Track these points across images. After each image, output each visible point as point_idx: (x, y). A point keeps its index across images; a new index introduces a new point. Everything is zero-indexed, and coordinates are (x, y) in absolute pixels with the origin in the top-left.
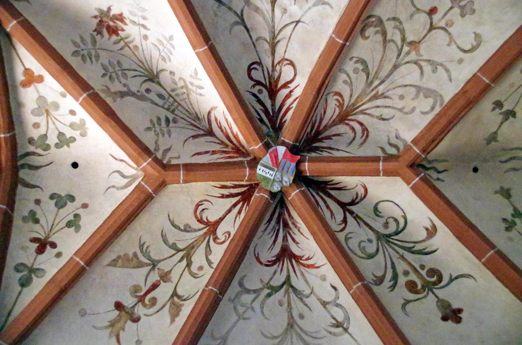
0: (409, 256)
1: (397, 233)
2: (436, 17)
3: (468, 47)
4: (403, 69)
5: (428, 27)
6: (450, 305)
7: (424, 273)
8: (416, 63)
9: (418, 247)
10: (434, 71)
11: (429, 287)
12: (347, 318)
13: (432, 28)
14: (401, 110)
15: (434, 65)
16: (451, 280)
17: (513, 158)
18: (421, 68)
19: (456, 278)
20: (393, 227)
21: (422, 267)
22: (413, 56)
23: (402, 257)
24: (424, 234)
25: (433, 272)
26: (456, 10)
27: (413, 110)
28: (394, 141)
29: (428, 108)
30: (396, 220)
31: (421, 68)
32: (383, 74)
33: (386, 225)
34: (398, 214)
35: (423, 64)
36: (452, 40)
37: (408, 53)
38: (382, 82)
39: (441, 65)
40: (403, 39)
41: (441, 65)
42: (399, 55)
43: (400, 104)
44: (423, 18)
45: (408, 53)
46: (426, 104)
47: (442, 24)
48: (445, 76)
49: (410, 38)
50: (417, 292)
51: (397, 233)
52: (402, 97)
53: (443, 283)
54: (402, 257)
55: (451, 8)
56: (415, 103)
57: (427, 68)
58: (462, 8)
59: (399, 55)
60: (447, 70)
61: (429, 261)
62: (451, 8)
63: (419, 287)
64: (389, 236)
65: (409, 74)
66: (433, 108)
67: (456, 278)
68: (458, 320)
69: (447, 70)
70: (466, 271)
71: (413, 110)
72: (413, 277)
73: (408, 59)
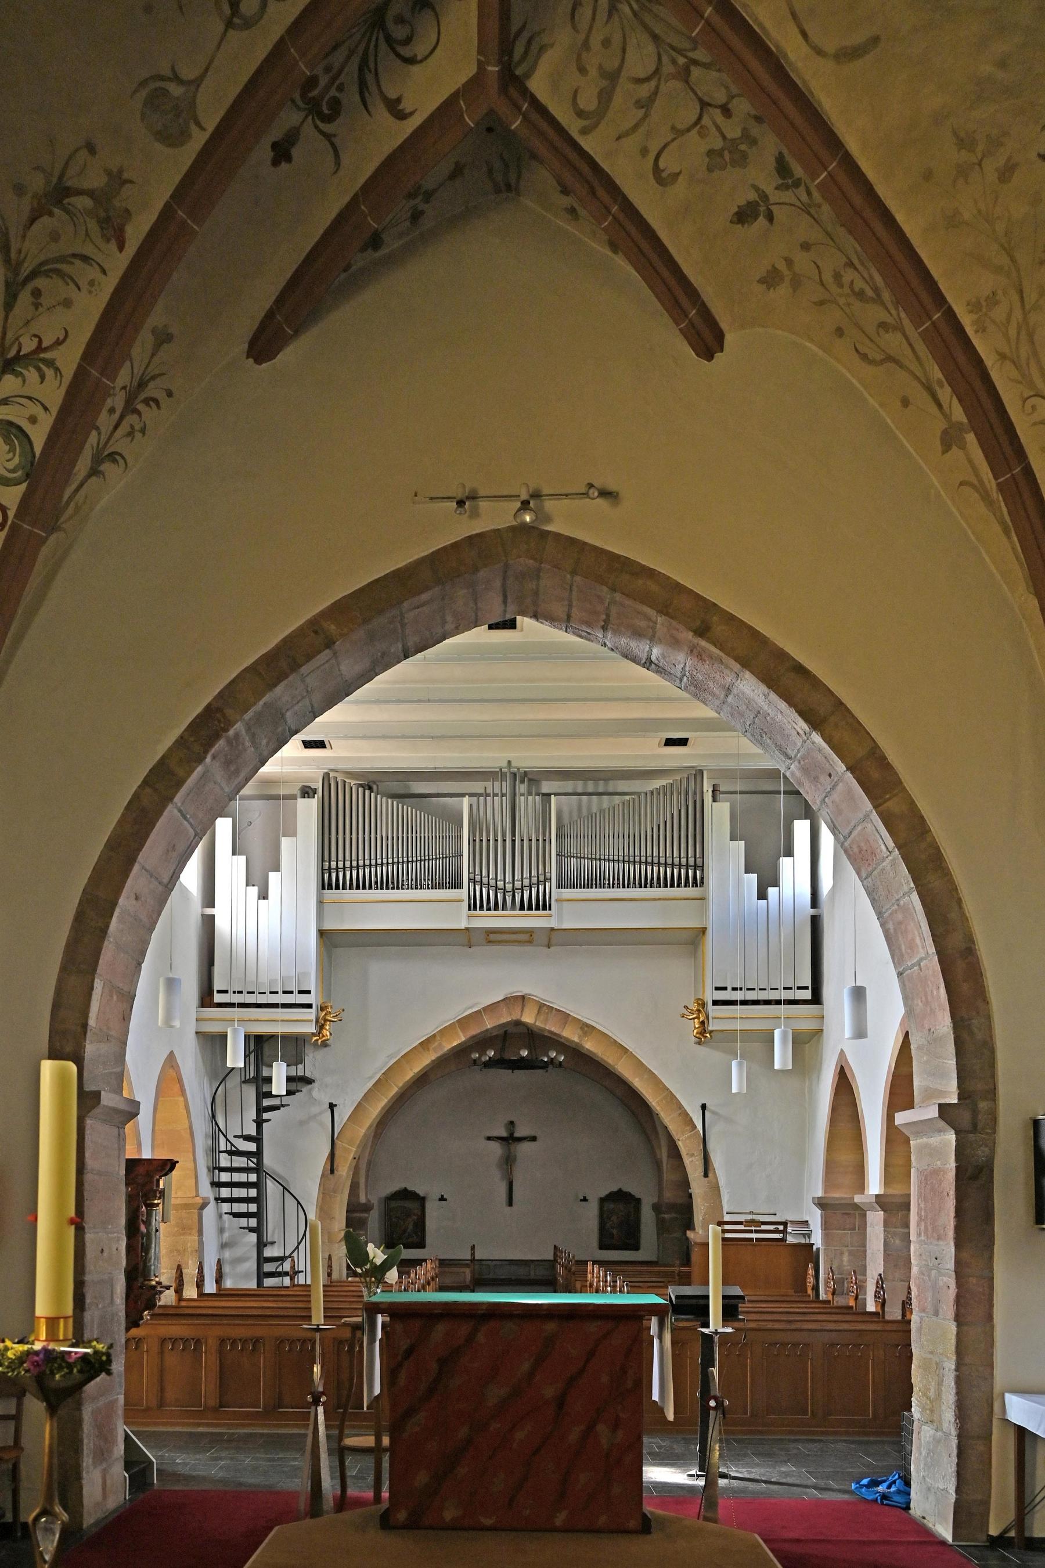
0: (356, 61)
1: (389, 39)
2: (717, 114)
3: (662, 164)
4: (651, 48)
5: (706, 99)
6: (293, 144)
7: (333, 92)
8: (657, 71)
9: (370, 78)
10: (639, 104)
11: (313, 108)
12: (248, 24)
13: (704, 105)
14: (586, 45)
15: (646, 104)
16: (328, 137)
17: (507, 166)
18: (647, 79)
19: (332, 144)
20: (399, 32)
21: (341, 88)
22: (668, 68)
23: (352, 52)
24: (392, 95)
25: (336, 106)
26: (718, 144)
27: (582, 70)
28: (534, 48)
29: (582, 104)
30: (408, 41)
31: (647, 79)
32: (648, 19)
33: (400, 20)
34: (420, 49)
35: (653, 83)
36: (679, 133)
37: (674, 62)
38: (635, 14)
39: (646, 116)
40: (695, 62)
41: (646, 116)
42: (673, 48)
43: (595, 42)
44: (720, 97)
45: (674, 62)
46: (588, 101)
47: (706, 121)
48: (628, 124)
49: (696, 72)
50: (303, 96)
51: (389, 39)
52: (606, 43)
53: (318, 122)
54: (352, 52)
55: (724, 137)
56: (593, 72)
57: (644, 91)
58: (720, 153)
59: (673, 48)
60: (636, 126)
61: (351, 97)
62: (724, 137)
63: (311, 95)
64: (383, 26)
65: (641, 58)
66: (580, 114)
67: (332, 144)
68: (276, 163)
69: (636, 126)
70: (346, 159)
71: (582, 70)
72: (323, 81)
73: (665, 59)
